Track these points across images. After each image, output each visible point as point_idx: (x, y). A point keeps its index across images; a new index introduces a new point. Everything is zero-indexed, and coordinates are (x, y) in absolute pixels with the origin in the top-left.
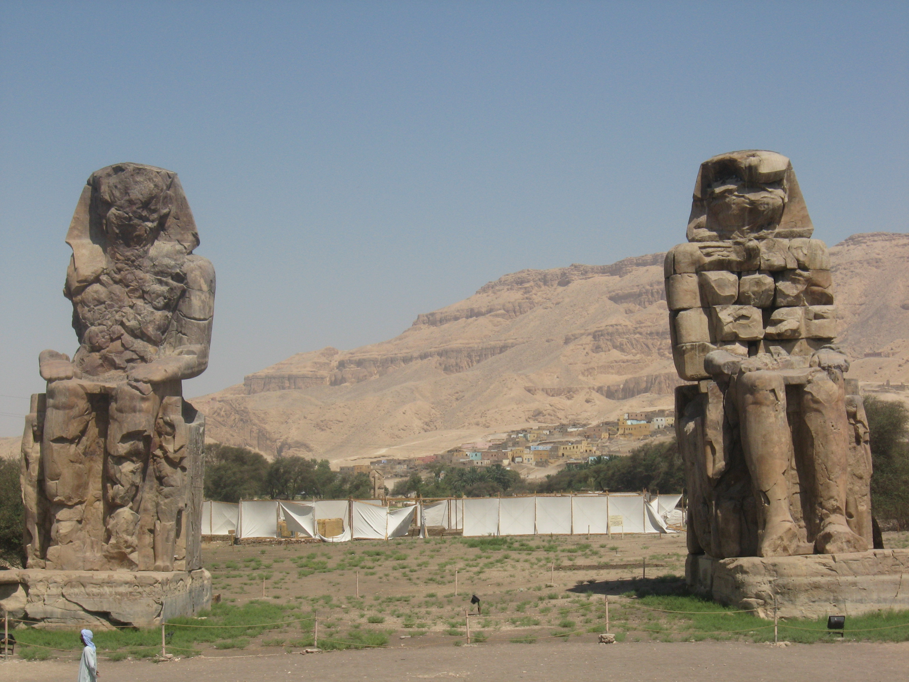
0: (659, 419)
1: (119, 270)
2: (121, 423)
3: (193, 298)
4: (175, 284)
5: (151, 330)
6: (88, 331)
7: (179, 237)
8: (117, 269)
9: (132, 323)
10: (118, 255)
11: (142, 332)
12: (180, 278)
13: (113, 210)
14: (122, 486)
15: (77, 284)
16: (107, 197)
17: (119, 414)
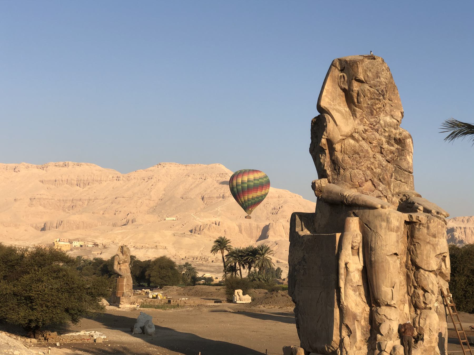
0: (76, 242)
1: (366, 131)
2: (434, 246)
3: (408, 157)
4: (396, 146)
5: (387, 177)
6: (348, 173)
7: (393, 113)
8: (365, 130)
9: (378, 171)
10: (366, 120)
11: (384, 179)
12: (400, 141)
13: (367, 87)
14: (434, 294)
15: (341, 137)
16: (361, 77)
17: (431, 238)
